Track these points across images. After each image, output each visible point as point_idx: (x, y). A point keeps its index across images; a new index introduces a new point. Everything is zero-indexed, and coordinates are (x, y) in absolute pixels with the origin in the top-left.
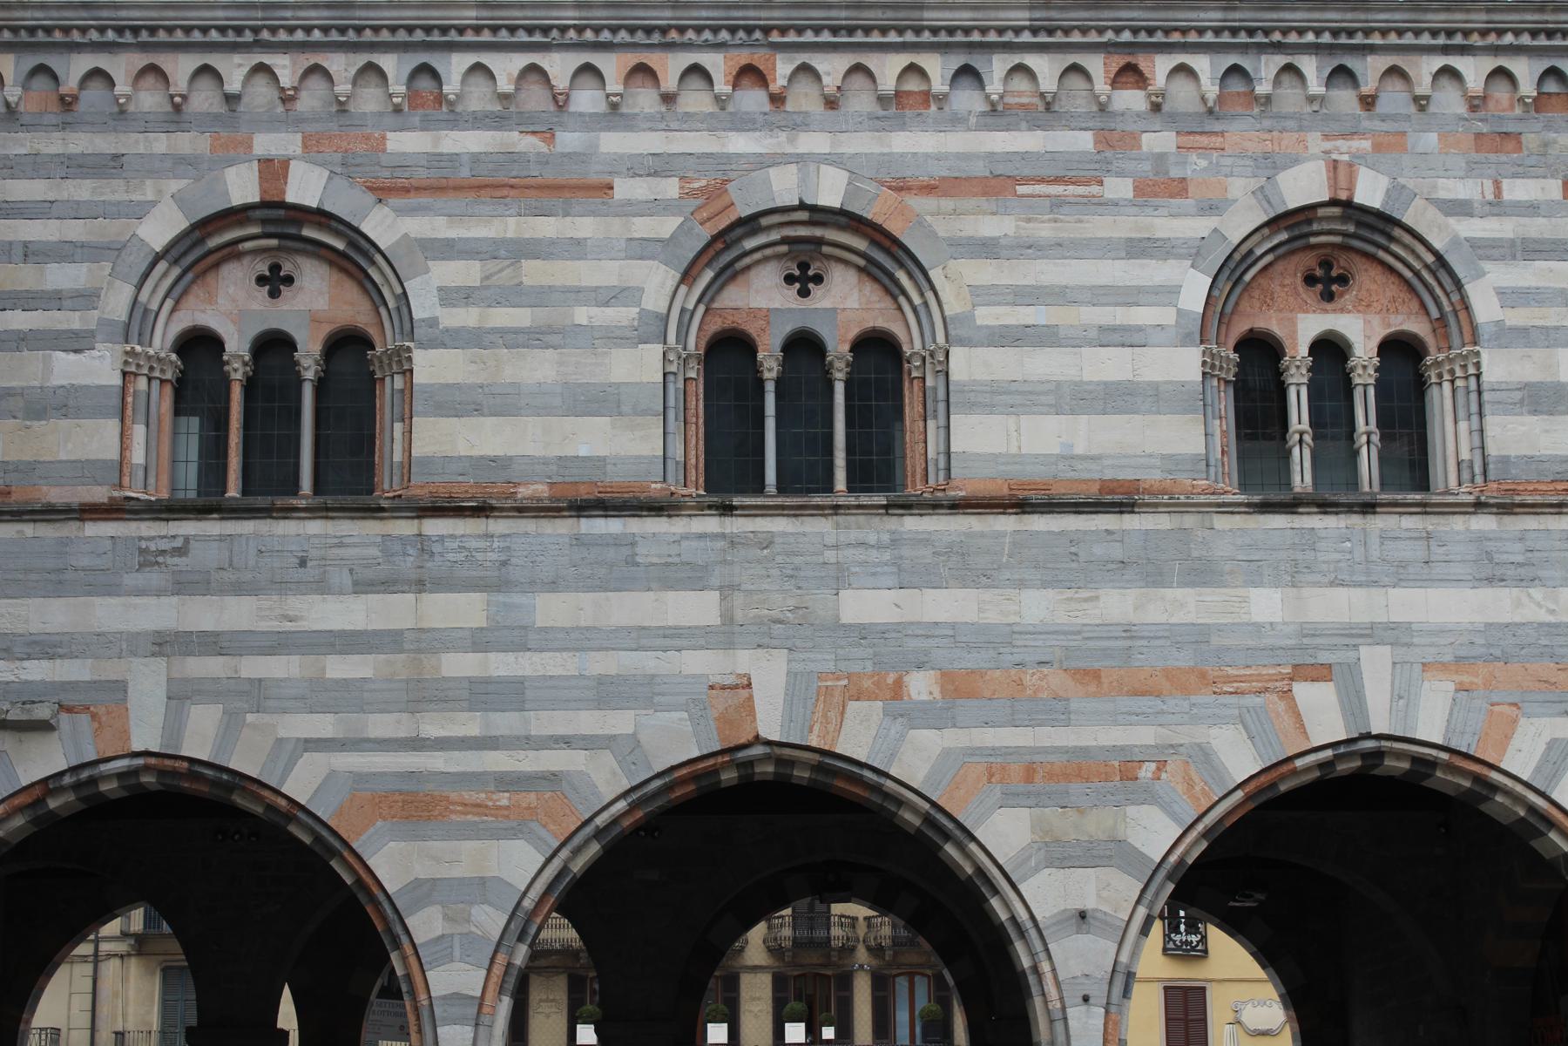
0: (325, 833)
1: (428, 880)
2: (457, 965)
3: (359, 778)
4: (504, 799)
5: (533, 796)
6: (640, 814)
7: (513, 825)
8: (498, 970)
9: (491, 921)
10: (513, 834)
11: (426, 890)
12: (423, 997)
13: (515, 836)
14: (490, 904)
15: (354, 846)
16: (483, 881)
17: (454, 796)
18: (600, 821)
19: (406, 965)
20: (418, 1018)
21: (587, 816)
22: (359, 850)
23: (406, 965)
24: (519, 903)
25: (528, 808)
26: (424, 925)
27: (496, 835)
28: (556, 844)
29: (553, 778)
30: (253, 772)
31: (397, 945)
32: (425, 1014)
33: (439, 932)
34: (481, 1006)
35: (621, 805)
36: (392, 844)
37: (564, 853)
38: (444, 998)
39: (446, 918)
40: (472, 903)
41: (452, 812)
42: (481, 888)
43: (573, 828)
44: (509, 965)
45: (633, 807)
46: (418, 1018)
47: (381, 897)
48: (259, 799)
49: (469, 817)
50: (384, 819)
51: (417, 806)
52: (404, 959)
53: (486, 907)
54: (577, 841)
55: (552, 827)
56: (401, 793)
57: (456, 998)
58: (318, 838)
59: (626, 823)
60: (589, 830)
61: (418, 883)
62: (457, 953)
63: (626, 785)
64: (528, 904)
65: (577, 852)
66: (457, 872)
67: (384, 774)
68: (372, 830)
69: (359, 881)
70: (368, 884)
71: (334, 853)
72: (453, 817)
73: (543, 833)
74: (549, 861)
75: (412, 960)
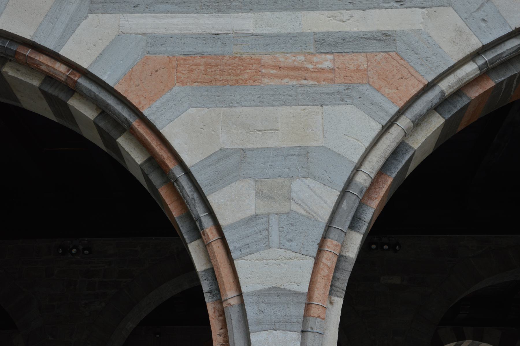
0: (111, 101)
1: (235, 151)
2: (274, 253)
3: (154, 40)
4: (327, 62)
5: (361, 58)
6: (490, 84)
7: (343, 89)
8: (328, 261)
9: (318, 199)
10: (342, 98)
11: (235, 163)
12: (230, 294)
13: (343, 102)
14: (315, 178)
15: (146, 112)
16: (305, 152)
17: (266, 59)
18: (447, 86)
19: (209, 257)
20: (224, 325)
21: (430, 78)
22: (152, 118)
23: (209, 257)
24: (350, 181)
25: (357, 71)
26: (231, 203)
27: (319, 101)
28: (394, 110)
29: (386, 37)
30: (25, 32)
31: (197, 233)
32: (233, 316)
33: (251, 212)
34: (308, 306)
35: (470, 69)
36: (192, 111)
37: (404, 122)
38: (259, 294)
39: (260, 194)
40: (292, 178)
41: (264, 75)
42: (304, 159)
43: (414, 91)
44: (340, 258)
45: (486, 72)
46: (224, 325)
47: (179, 173)
48: (33, 68)
49: (285, 81)
50: (183, 84)
51: (221, 71)
52: (206, 247)
53: (310, 182)
54: (419, 107)
55: (387, 91)
56: (203, 55)
57: (276, 293)
58: (104, 112)
59: (475, 93)
60: (432, 96)
61: (223, 154)
62: (275, 237)
63: (476, 44)
64: (363, 180)
65: (418, 123)
66: (271, 142)
67: (184, 36)
68: (167, 96)
69: (153, 161)
70: (163, 161)
71: (123, 127)
72: (266, 81)
73: (377, 97)
74: (386, 129)
75: (217, 248)
